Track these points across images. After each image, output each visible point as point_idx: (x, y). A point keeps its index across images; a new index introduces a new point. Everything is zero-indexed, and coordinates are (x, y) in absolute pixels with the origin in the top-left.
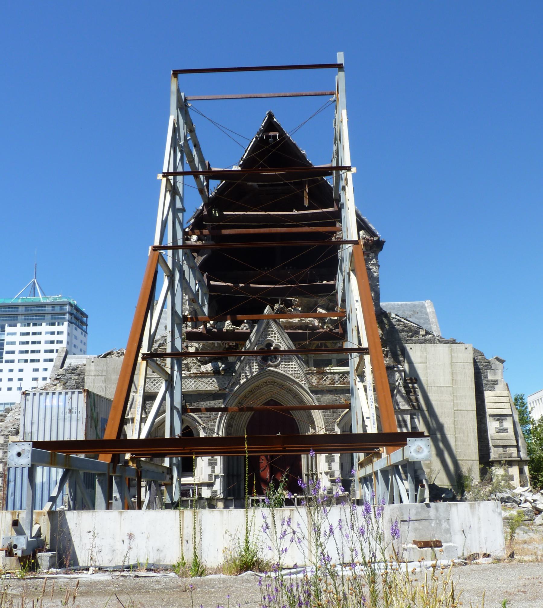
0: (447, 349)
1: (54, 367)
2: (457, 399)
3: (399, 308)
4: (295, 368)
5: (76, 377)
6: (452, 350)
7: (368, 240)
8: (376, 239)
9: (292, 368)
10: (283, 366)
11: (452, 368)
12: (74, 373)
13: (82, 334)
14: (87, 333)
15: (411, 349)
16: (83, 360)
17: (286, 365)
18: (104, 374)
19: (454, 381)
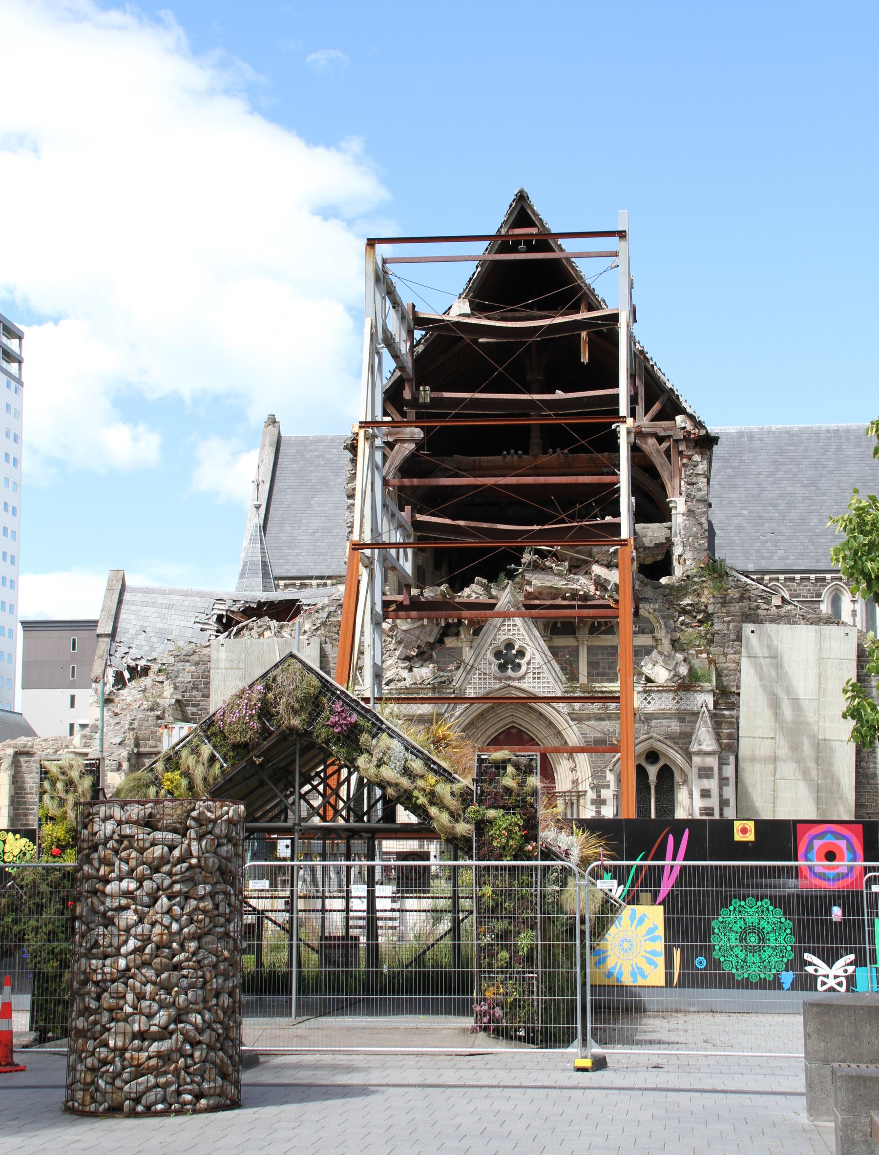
0: (813, 634)
1: (102, 611)
2: (825, 721)
3: (829, 438)
4: (549, 683)
5: (193, 668)
6: (821, 636)
7: (689, 432)
8: (703, 432)
9: (544, 683)
10: (531, 680)
11: (819, 668)
12: (188, 661)
13: (8, 386)
14: (22, 384)
15: (753, 632)
16: (157, 596)
17: (534, 678)
18: (242, 665)
19: (822, 690)
